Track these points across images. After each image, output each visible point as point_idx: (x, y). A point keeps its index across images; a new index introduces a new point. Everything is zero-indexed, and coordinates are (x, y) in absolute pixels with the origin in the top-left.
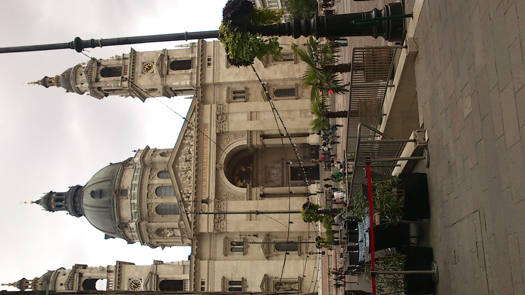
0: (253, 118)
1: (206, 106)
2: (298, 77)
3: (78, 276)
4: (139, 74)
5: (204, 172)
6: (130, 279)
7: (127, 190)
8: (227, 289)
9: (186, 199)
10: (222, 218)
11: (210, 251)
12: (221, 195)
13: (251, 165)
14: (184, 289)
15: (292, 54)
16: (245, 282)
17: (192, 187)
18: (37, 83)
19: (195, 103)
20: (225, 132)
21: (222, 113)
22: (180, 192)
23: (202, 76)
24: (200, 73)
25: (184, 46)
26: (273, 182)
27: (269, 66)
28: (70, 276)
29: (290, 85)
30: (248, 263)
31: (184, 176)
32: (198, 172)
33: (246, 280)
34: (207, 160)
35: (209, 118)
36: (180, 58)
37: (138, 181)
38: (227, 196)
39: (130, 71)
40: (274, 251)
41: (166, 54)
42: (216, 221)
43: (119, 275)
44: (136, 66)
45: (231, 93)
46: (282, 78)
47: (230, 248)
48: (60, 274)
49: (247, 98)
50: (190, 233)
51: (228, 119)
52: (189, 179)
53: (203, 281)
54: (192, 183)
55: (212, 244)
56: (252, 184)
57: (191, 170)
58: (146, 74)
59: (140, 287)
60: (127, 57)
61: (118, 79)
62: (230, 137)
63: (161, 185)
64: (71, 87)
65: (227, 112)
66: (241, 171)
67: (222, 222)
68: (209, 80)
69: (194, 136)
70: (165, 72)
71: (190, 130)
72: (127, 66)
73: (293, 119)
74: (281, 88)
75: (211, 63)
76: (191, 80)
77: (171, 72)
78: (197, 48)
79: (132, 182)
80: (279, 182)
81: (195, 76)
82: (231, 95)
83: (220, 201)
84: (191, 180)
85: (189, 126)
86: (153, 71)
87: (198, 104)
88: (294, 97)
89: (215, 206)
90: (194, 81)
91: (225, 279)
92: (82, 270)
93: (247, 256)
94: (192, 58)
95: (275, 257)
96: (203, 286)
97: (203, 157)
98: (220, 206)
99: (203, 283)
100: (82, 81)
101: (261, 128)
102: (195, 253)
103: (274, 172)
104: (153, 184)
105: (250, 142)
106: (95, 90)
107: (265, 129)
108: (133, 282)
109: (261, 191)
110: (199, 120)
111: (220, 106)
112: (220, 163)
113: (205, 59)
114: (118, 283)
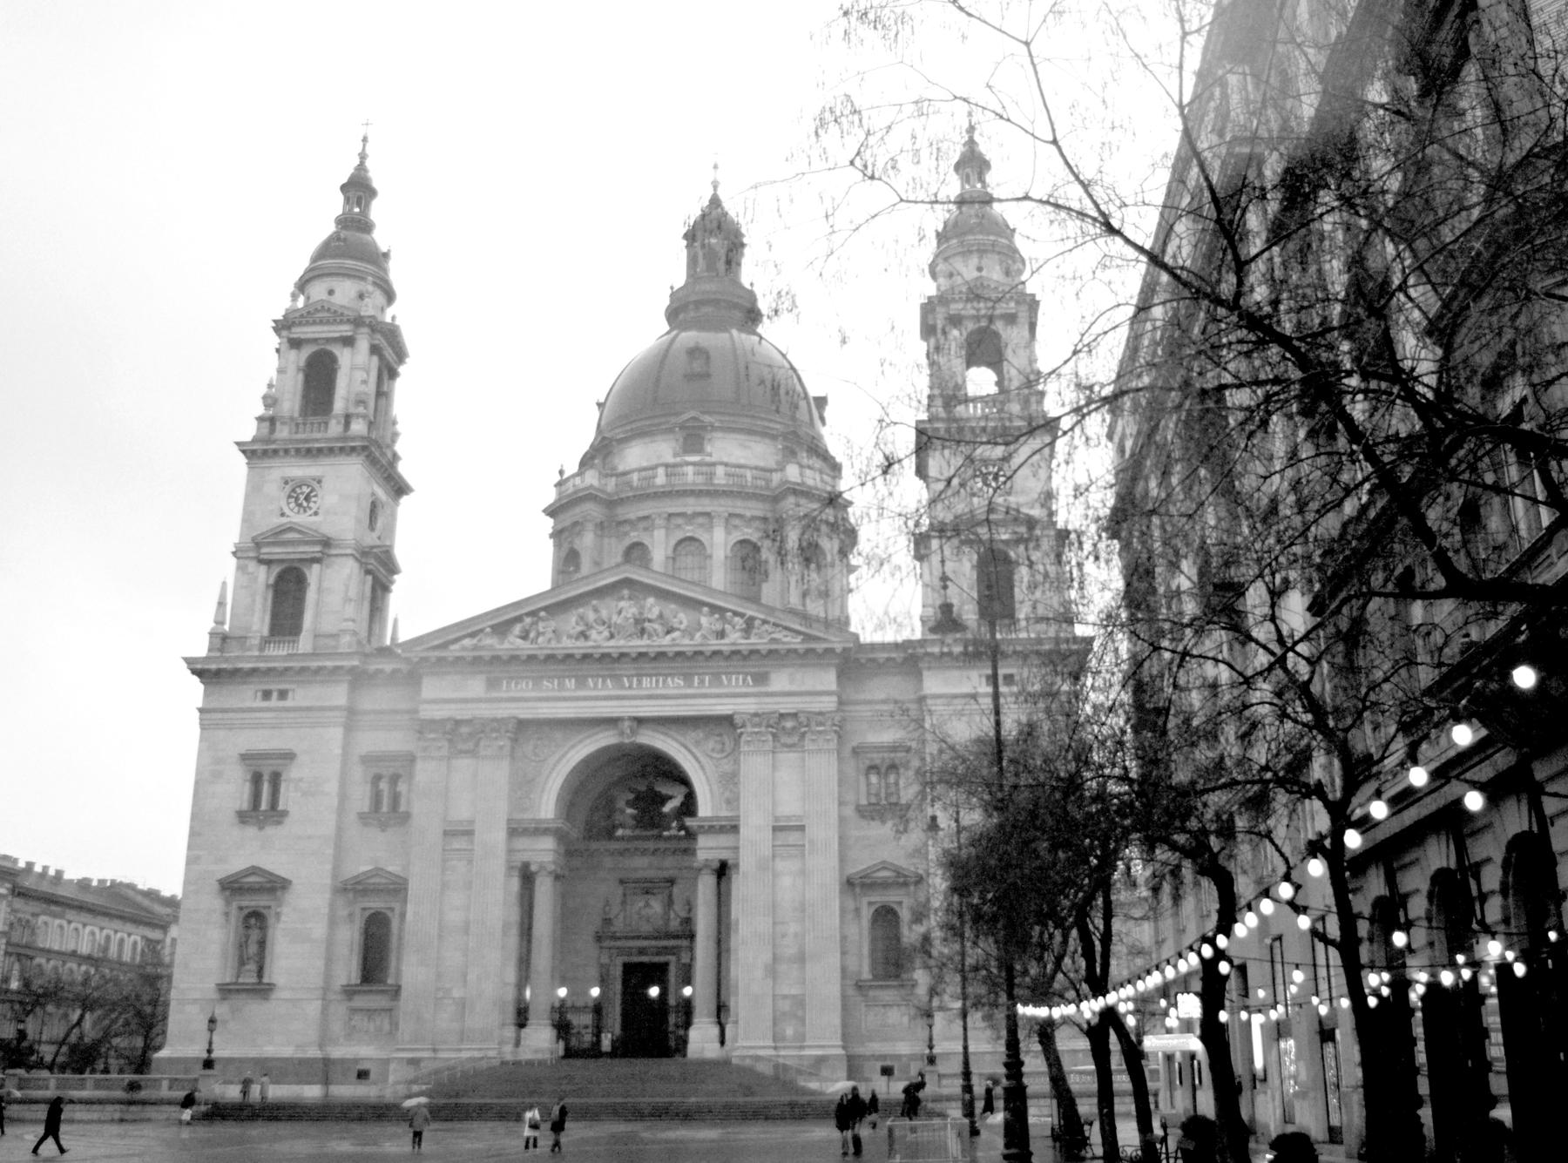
0: (779, 834)
3: (345, 334)
7: (700, 451)
9: (517, 629)
10: (461, 746)
12: (539, 739)
14: (273, 639)
17: (553, 644)
21: (803, 730)
22: (545, 609)
28: (346, 312)
30: (328, 827)
31: (591, 616)
33: (279, 823)
35: (788, 688)
37: (724, 482)
40: (364, 909)
42: (449, 726)
43: (331, 450)
53: (290, 694)
56: (622, 838)
57: (612, 636)
63: (709, 551)
65: (808, 745)
66: (665, 799)
67: (446, 744)
69: (723, 641)
73: (772, 972)
79: (722, 463)
84: (577, 638)
85: (757, 623)
87: (832, 651)
92: (363, 344)
95: (343, 912)
96: (275, 695)
97: (656, 675)
98: (494, 735)
99: (283, 695)
101: (747, 863)
102: (372, 667)
103: (657, 906)
104: (712, 527)
105: (702, 827)
109: (542, 867)
110: (776, 656)
111: (829, 723)
114: (309, 451)
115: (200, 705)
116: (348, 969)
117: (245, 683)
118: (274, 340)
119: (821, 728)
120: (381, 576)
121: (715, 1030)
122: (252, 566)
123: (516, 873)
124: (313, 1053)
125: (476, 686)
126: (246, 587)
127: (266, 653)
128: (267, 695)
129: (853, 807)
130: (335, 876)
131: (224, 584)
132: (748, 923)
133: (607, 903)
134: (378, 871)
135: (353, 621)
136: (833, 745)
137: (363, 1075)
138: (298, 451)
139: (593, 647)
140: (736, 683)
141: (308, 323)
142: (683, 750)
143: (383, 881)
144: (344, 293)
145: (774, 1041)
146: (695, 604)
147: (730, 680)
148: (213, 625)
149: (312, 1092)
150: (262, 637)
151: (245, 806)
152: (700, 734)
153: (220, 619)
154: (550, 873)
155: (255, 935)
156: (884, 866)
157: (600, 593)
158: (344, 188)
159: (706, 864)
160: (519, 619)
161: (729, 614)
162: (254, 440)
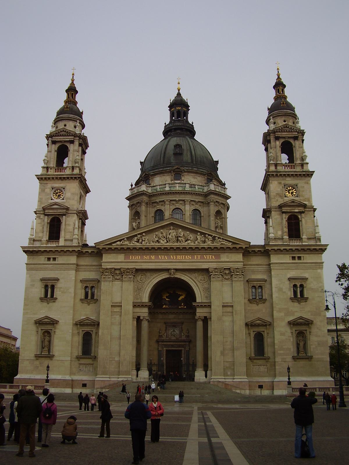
0: (224, 308)
1: (241, 256)
2: (277, 360)
3: (71, 139)
4: (283, 182)
5: (166, 257)
6: (64, 189)
8: (47, 283)
11: (86, 266)
12: (142, 275)
13: (185, 307)
15: (306, 354)
16: (53, 300)
17: (148, 244)
18: (279, 77)
19: (243, 244)
20: (211, 278)
21: (232, 274)
23: (278, 251)
24: (282, 248)
25: (317, 229)
26: (165, 331)
27: (291, 327)
29: (268, 351)
31: (161, 235)
32: (166, 250)
33: (54, 302)
34: (179, 259)
35: (226, 260)
36: (302, 226)
38: (140, 282)
39: (286, 172)
41: (307, 210)
42: (113, 270)
43: (68, 178)
44: (292, 178)
45: (259, 284)
46: (275, 342)
47: (88, 285)
48: (75, 122)
49: (254, 301)
50: (101, 244)
51: (226, 280)
52: (157, 241)
53: (56, 259)
54: (152, 244)
55: (93, 267)
57: (167, 242)
58: (283, 189)
59: (57, 199)
60: (305, 169)
61: (278, 159)
62: (205, 284)
64: (272, 112)
68: (275, 259)
69: (205, 244)
70: (284, 209)
71: (212, 239)
72: (294, 169)
73: (223, 353)
74: (265, 340)
75: (295, 260)
76: (275, 238)
77: (285, 217)
78: (315, 244)
80: (165, 337)
81: (280, 243)
82: (257, 284)
83: (134, 274)
84: (156, 242)
86: (287, 197)
88: (253, 355)
89: (127, 269)
90: (273, 241)
91: (57, 281)
92: (77, 143)
93: (79, 304)
94: (302, 238)
95: (76, 332)
96: (52, 259)
98: (128, 274)
99: (54, 259)
100: (277, 123)
101: (214, 317)
102: (84, 251)
106: (268, 137)
107: (212, 322)
108: (62, 191)
110: (223, 249)
112: (176, 273)
113: (301, 254)
114: (60, 178)
115: (26, 263)
116: (78, 351)
117: (40, 255)
118: (46, 142)
119: (238, 274)
120: (83, 220)
121: (204, 373)
122: (42, 216)
123: (136, 320)
124: (68, 377)
125: (121, 257)
126: (40, 223)
127: (48, 246)
128: (49, 259)
129: (247, 299)
130: (73, 320)
131: (33, 222)
132: (215, 338)
133: (160, 331)
134: (88, 319)
135: (77, 235)
136: (242, 279)
137: (84, 385)
138: (57, 178)
139: (161, 245)
140: (209, 257)
141: (58, 136)
142: (191, 280)
143: (89, 322)
144: (70, 126)
145: (224, 376)
146: (195, 232)
147: (207, 257)
148: (30, 236)
149: (68, 391)
150: (47, 240)
151: (43, 296)
152: (196, 275)
153: (32, 234)
154: (147, 320)
155: (47, 338)
156: (259, 319)
157: (162, 227)
158: (67, 91)
159: (200, 318)
160: (136, 236)
161: (207, 235)
162: (41, 175)
